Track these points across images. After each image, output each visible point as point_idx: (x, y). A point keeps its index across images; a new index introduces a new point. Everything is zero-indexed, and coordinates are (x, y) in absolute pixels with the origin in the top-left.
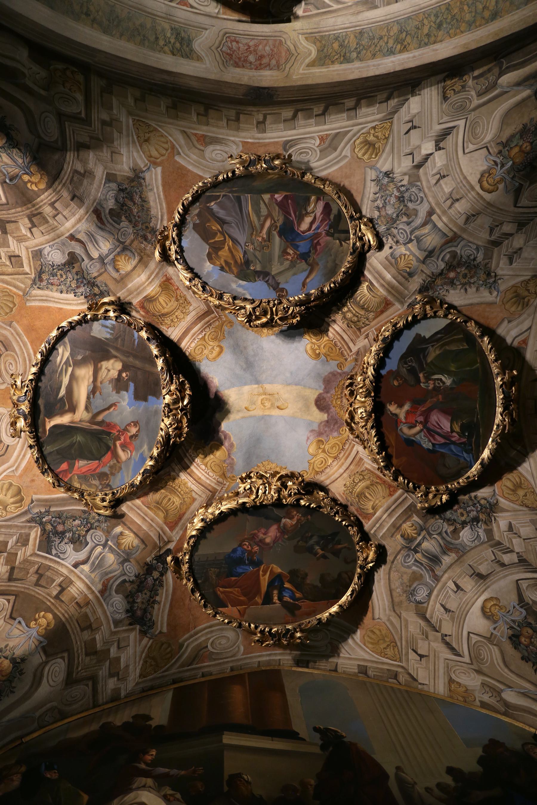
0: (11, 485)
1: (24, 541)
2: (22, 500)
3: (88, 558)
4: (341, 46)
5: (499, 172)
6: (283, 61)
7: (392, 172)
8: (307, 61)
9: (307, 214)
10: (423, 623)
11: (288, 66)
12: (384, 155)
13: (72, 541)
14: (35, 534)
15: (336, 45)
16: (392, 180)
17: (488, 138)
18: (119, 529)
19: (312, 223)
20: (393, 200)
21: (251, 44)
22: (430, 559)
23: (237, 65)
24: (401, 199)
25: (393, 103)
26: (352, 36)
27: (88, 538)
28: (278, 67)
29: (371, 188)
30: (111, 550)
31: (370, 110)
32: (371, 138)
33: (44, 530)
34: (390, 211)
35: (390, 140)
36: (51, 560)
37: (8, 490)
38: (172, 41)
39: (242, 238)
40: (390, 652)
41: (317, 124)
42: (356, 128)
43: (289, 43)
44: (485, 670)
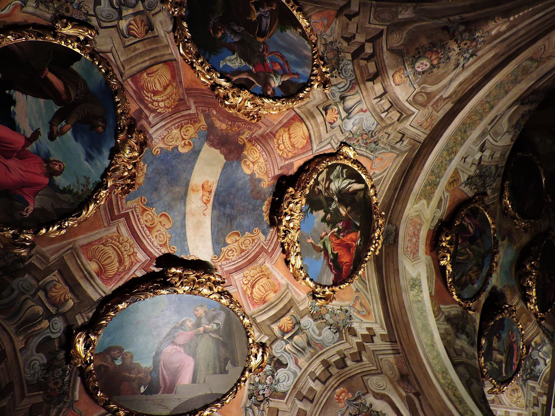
0: (510, 394)
1: (533, 388)
2: (516, 389)
3: (543, 359)
4: (430, 185)
6: (419, 221)
7: (470, 176)
8: (426, 207)
9: (468, 227)
11: (423, 219)
13: (535, 366)
14: (531, 383)
15: (428, 188)
16: (472, 177)
18: (533, 343)
19: (472, 227)
21: (408, 238)
23: (418, 250)
26: (430, 177)
27: (535, 358)
28: (421, 225)
30: (541, 348)
33: (529, 379)
35: (459, 171)
36: (542, 376)
37: (512, 396)
38: (417, 291)
39: (470, 266)
43: (414, 215)
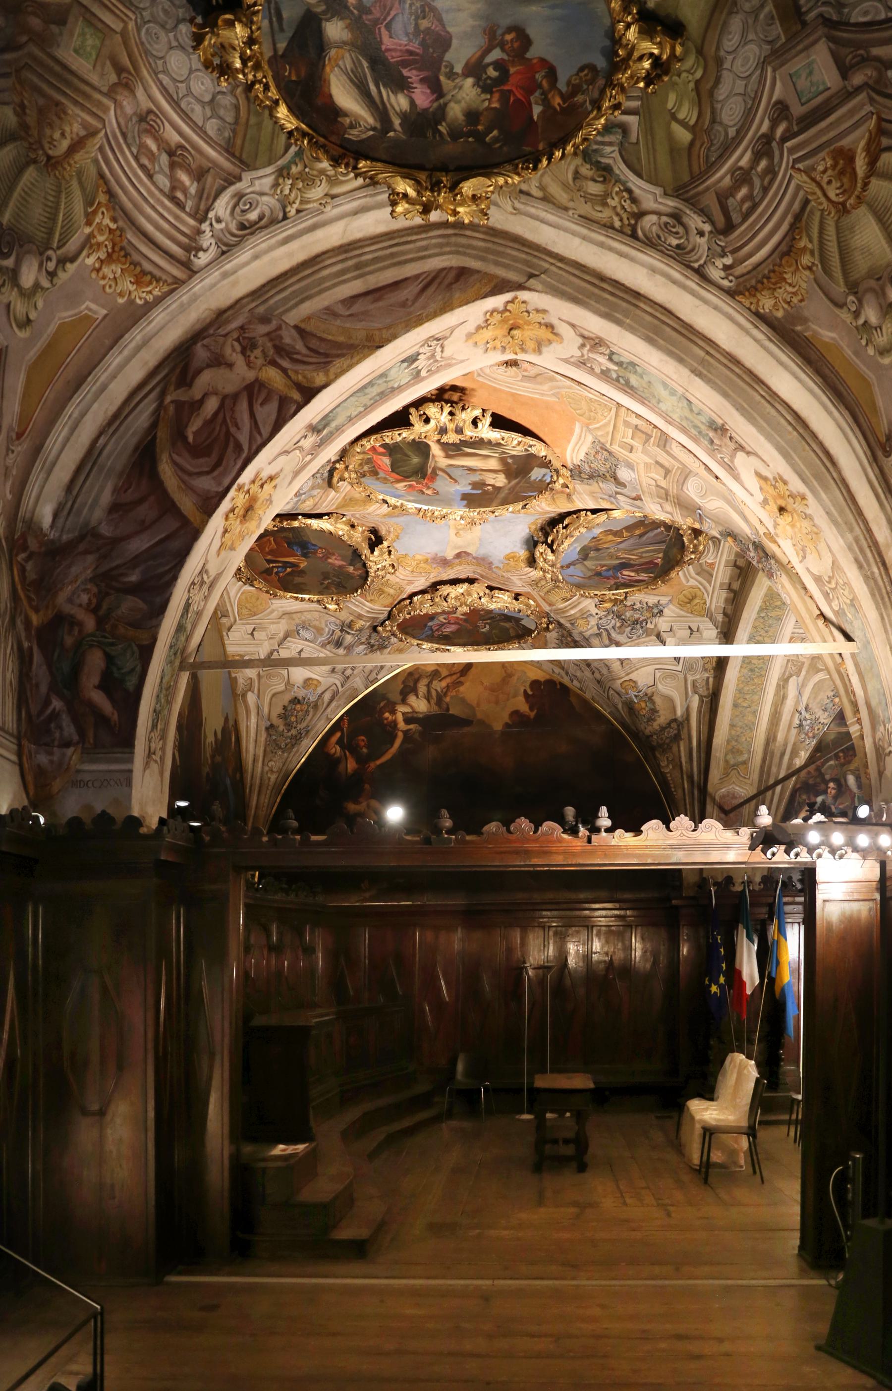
5: (632, 693)
10: (281, 635)
12: (677, 610)
17: (660, 687)
20: (636, 616)
22: (338, 641)
24: (636, 622)
25: (720, 618)
29: (652, 600)
31: (722, 600)
32: (696, 601)
34: (628, 614)
40: (245, 611)
41: (727, 561)
42: (710, 589)
44: (263, 680)
